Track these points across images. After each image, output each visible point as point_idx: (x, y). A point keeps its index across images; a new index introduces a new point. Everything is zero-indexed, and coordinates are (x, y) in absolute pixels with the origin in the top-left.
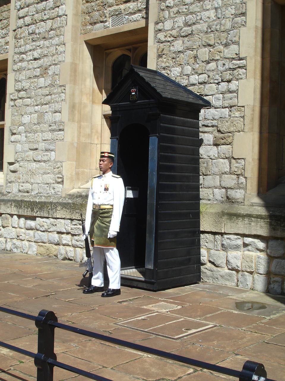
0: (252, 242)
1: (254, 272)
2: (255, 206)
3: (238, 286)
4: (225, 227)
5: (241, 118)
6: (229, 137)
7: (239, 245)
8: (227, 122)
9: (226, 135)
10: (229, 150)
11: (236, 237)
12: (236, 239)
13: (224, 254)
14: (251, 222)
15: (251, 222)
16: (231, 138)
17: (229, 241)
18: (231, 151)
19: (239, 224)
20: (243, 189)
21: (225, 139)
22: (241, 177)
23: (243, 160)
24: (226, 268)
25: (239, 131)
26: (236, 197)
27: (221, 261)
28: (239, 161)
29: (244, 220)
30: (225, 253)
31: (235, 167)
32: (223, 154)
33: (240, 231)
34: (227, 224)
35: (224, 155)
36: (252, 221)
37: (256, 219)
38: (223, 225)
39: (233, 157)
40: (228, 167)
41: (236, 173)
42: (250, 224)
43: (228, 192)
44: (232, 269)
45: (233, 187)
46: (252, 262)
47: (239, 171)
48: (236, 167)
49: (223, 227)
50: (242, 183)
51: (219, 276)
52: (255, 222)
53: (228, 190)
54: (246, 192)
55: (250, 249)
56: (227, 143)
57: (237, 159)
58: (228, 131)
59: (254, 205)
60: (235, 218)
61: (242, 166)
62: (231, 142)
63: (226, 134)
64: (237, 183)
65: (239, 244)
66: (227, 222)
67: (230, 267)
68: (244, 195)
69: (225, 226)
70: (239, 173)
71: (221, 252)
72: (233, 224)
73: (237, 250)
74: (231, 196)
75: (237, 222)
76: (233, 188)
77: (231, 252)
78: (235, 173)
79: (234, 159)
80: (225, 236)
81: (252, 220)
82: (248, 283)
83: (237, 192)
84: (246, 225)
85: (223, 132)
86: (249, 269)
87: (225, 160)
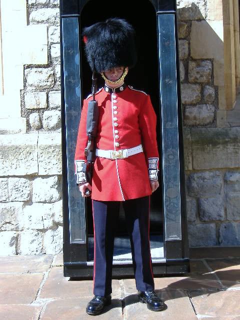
2: (234, 127)
14: (237, 150)
26: (201, 117)
28: (204, 63)
45: (194, 102)
48: (198, 73)
50: (210, 95)
60: (211, 145)
68: (215, 113)
75: (214, 152)
79: (194, 60)
84: (230, 155)
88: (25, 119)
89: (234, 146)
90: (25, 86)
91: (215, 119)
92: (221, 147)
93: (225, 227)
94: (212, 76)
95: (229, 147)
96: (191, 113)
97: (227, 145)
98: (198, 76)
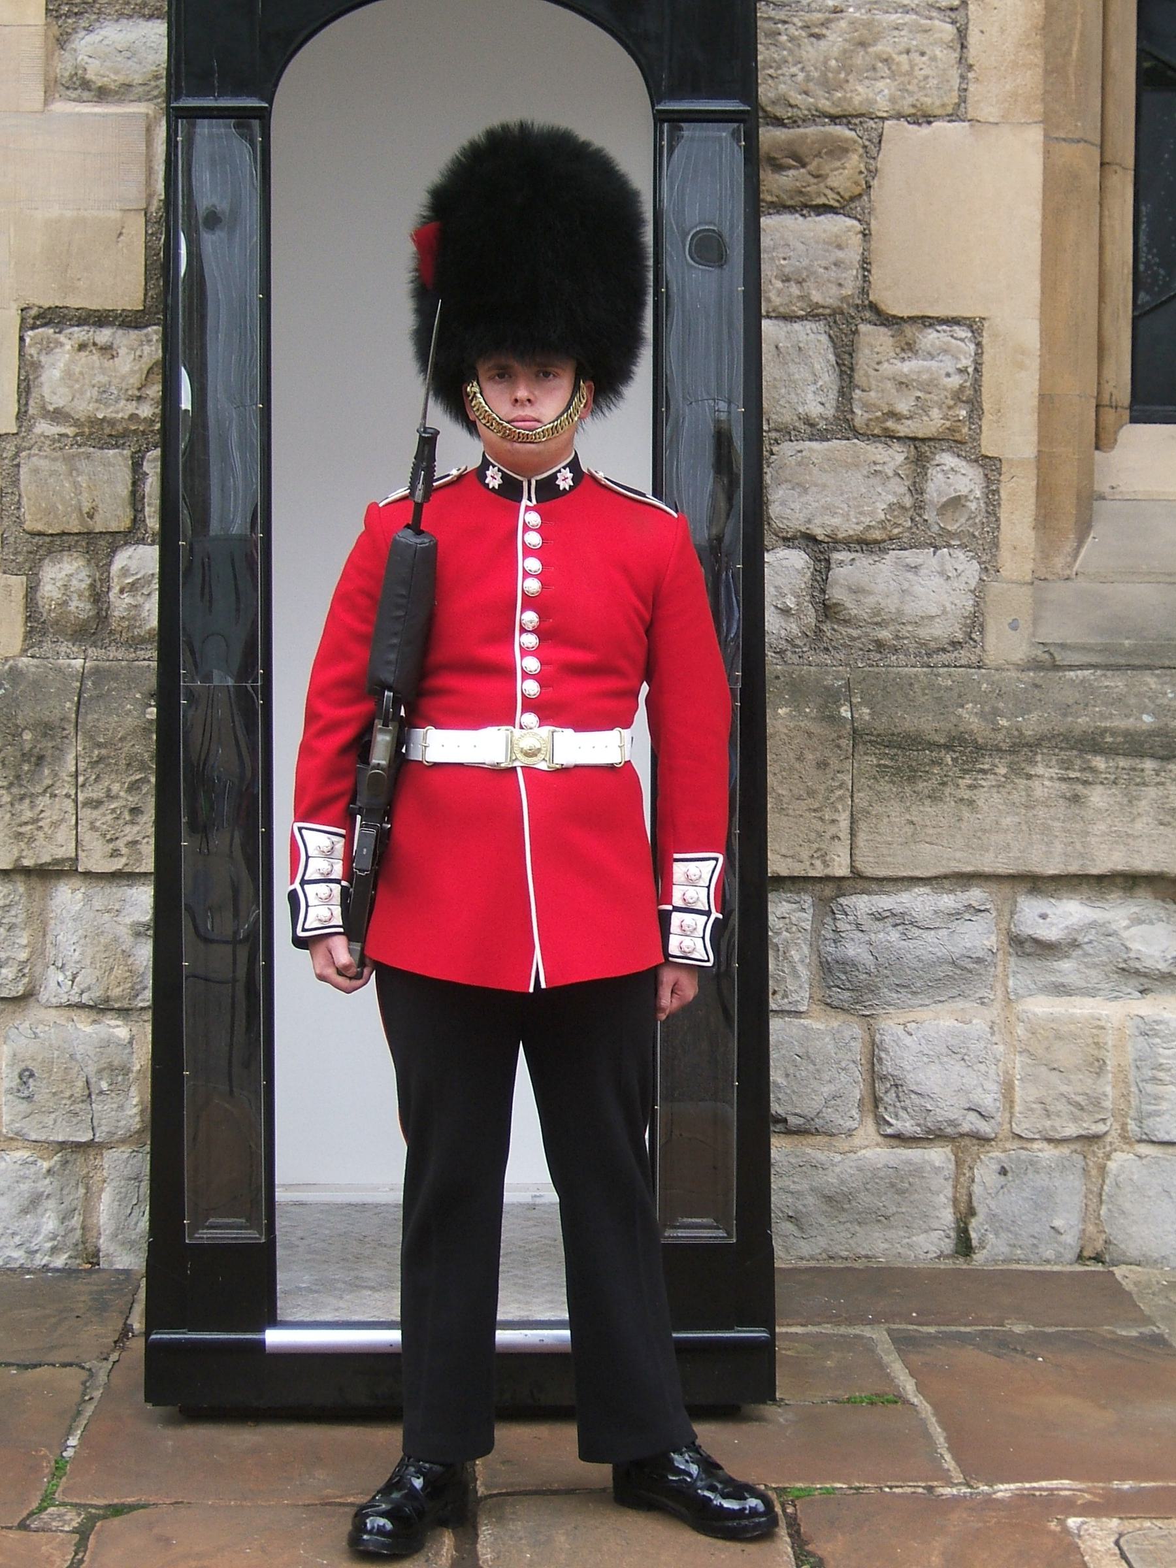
0: (1093, 925)
1: (1109, 1139)
2: (1071, 667)
3: (964, 1246)
4: (862, 837)
5: (934, 14)
6: (839, 150)
7: (979, 961)
8: (812, 35)
9: (806, 136)
10: (840, 254)
11: (948, 901)
12: (956, 915)
13: (847, 1034)
14: (1079, 788)
15: (1085, 783)
16: (854, 161)
17: (894, 935)
18: (852, 255)
19: (980, 803)
20: (963, 546)
21: (804, 165)
22: (948, 460)
23: (962, 332)
24: (868, 1130)
25: (923, 118)
26: (912, 609)
27: (827, 1090)
28: (931, 338)
29: (1029, 777)
30: (855, 1029)
31: (889, 385)
32: (786, 280)
33: (989, 857)
34: (877, 809)
35: (795, 290)
36: (1088, 776)
37: (1123, 762)
38: (844, 823)
39: (874, 307)
40: (829, 379)
41: (903, 429)
42: (1076, 799)
43: (837, 573)
44: (934, 1136)
45: (877, 535)
46: (1098, 1066)
47: (935, 413)
48: (903, 384)
49: (845, 835)
50: (956, 503)
51: (811, 1200)
52: (1115, 783)
53: (836, 556)
54: (989, 568)
55: (1074, 980)
56: (821, 201)
57: (912, 319)
58: (825, 105)
59: (1061, 657)
61: (955, 381)
62: (857, 190)
63: (811, 131)
64: (908, 501)
65: (980, 954)
66: (880, 797)
67: (906, 1125)
68: (979, 594)
69: (863, 825)
70: (933, 423)
71: (820, 1026)
72: (929, 809)
73: (955, 992)
74: (870, 600)
75: (967, 794)
76: (876, 542)
77: (911, 1016)
78: (890, 424)
79: (885, 320)
80: (861, 904)
81: (1093, 770)
82: (1058, 1223)
83: (915, 569)
84: (1041, 812)
85: (780, 111)
86: (1075, 1119)
87: (797, 326)
88: (18, 583)
89: (1067, 765)
90: (21, 416)
91: (975, 623)
92: (1002, 770)
93: (1003, 1172)
94: (975, 406)
95: (1040, 770)
96: (857, 591)
97: (1032, 762)
98: (903, 406)
